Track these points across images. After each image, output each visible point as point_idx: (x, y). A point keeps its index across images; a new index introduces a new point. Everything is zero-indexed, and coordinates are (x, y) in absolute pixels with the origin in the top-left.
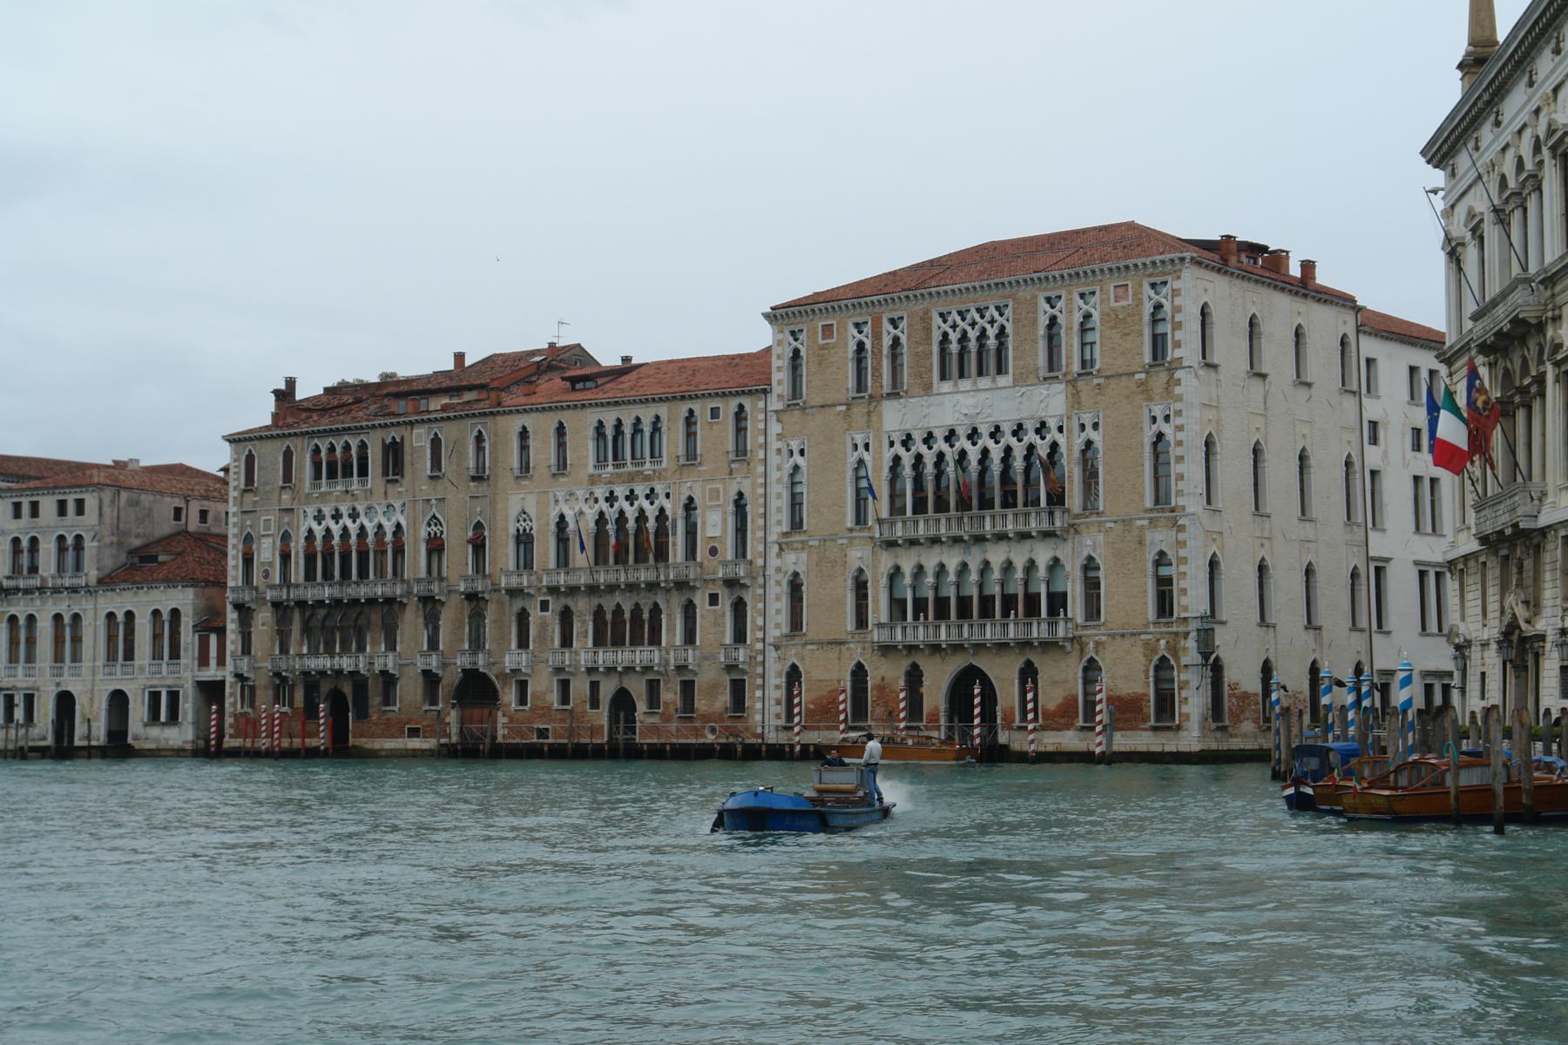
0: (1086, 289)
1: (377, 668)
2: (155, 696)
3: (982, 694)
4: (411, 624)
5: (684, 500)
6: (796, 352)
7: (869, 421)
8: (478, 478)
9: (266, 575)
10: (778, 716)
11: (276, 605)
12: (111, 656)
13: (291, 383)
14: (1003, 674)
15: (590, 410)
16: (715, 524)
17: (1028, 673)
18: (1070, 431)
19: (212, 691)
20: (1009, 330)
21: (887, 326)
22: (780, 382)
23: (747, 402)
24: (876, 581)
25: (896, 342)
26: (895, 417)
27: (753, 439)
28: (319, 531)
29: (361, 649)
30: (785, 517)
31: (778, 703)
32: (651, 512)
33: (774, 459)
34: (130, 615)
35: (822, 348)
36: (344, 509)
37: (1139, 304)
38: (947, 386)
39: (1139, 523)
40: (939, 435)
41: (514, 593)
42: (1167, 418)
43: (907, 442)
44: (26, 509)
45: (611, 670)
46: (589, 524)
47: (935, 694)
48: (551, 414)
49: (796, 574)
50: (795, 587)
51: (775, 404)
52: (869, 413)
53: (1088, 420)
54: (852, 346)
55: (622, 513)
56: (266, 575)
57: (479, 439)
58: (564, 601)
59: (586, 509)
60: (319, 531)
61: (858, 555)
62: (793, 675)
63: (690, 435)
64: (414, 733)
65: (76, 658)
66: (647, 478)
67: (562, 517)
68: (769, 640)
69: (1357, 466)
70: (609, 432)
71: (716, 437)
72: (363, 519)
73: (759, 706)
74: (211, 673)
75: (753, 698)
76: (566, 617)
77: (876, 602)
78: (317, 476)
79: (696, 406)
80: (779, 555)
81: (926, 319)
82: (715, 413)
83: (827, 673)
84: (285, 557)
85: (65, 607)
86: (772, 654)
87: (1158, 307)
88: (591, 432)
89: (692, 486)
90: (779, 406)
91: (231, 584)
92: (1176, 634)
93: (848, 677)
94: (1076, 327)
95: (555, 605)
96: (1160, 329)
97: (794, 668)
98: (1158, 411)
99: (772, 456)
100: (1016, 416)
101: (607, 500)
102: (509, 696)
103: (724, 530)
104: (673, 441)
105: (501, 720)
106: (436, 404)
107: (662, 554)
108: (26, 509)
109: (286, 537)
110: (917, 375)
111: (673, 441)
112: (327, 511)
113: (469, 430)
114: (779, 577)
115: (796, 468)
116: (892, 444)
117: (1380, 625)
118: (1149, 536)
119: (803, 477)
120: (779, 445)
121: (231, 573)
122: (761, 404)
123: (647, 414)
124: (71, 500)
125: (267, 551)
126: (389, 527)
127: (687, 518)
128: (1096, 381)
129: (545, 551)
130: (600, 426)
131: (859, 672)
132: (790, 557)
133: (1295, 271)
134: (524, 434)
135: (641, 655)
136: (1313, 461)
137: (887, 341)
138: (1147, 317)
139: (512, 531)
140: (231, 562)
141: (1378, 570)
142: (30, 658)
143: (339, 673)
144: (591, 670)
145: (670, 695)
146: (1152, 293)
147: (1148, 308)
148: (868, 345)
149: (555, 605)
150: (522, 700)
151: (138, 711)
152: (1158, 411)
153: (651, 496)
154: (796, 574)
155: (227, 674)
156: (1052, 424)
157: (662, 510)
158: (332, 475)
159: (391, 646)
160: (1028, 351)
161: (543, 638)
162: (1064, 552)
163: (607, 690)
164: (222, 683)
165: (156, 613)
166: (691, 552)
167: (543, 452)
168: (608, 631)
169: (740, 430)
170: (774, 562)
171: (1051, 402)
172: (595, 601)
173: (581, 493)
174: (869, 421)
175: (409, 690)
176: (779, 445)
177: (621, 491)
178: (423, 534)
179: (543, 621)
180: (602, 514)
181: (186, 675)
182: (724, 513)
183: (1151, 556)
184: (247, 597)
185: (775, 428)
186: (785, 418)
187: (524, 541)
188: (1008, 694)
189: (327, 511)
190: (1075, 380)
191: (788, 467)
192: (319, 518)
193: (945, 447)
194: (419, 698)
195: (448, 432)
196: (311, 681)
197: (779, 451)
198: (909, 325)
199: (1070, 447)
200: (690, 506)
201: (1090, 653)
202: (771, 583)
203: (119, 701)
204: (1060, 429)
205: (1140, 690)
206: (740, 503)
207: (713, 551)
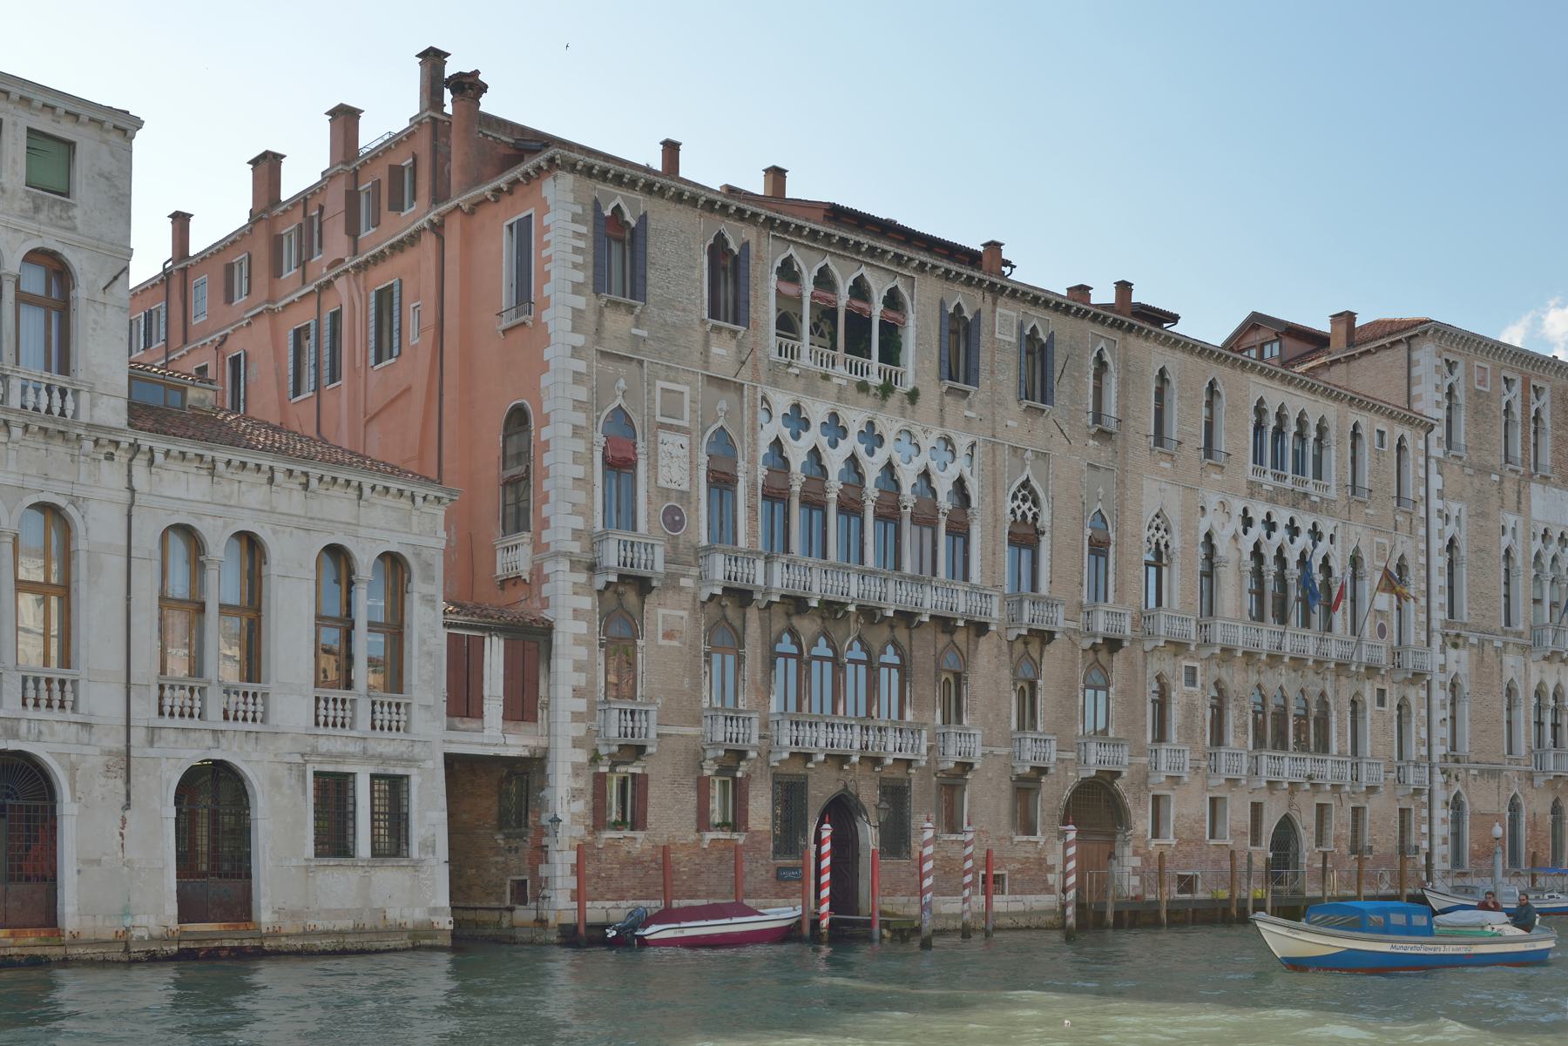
8: (1104, 435)
9: (673, 519)
15: (1254, 377)
31: (1445, 842)
33: (1436, 523)
48: (1202, 363)
62: (1456, 805)
66: (1314, 508)
68: (1436, 759)
80: (1443, 651)
102: (1142, 822)
114: (1442, 677)
126: (943, 485)
129: (1181, 581)
131: (1514, 807)
132: (1452, 652)
151: (280, 825)
168: (1274, 729)
173: (1237, 506)
175: (986, 801)
189: (817, 412)
194: (1005, 819)
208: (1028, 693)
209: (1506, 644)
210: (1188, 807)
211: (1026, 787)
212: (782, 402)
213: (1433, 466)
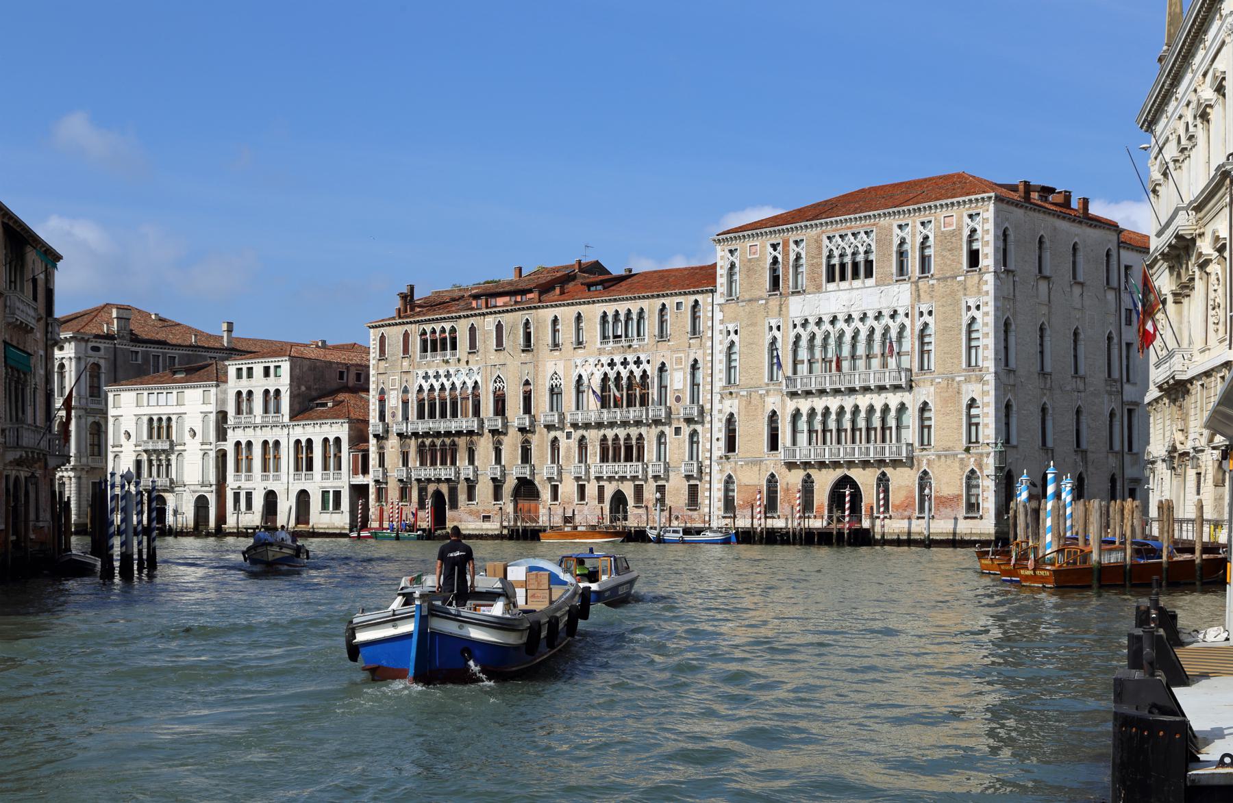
0: (925, 220)
1: (462, 477)
2: (325, 494)
3: (851, 494)
4: (484, 446)
5: (658, 365)
6: (733, 266)
7: (781, 310)
9: (394, 415)
10: (719, 509)
11: (400, 435)
12: (297, 468)
13: (412, 288)
14: (866, 479)
16: (678, 380)
17: (883, 481)
18: (913, 316)
19: (359, 491)
20: (873, 248)
21: (793, 246)
22: (722, 285)
23: (699, 297)
24: (784, 419)
25: (798, 257)
26: (798, 307)
27: (704, 324)
28: (426, 387)
29: (453, 463)
30: (723, 375)
32: (638, 373)
33: (718, 337)
34: (309, 441)
35: (750, 260)
36: (442, 372)
37: (960, 229)
38: (832, 286)
39: (958, 379)
40: (826, 319)
41: (550, 427)
42: (978, 307)
43: (805, 324)
44: (244, 373)
45: (610, 479)
46: (596, 383)
47: (821, 496)
49: (732, 415)
50: (730, 420)
51: (719, 299)
52: (781, 305)
53: (924, 309)
54: (770, 260)
55: (619, 373)
56: (394, 415)
57: (527, 323)
58: (581, 432)
59: (595, 370)
60: (426, 387)
61: (772, 402)
62: (729, 480)
63: (662, 322)
64: (486, 518)
65: (277, 469)
66: (635, 350)
67: (580, 376)
69: (1116, 340)
70: (610, 319)
71: (679, 322)
72: (454, 379)
73: (707, 502)
74: (360, 480)
75: (703, 495)
76: (582, 442)
77: (784, 433)
78: (424, 350)
79: (667, 301)
80: (721, 402)
81: (818, 241)
82: (679, 305)
83: (751, 479)
84: (405, 403)
85: (271, 435)
86: (715, 467)
87: (974, 231)
88: (598, 320)
89: (663, 354)
90: (722, 301)
91: (372, 421)
92: (982, 454)
93: (765, 483)
94: (918, 245)
95: (576, 435)
96: (975, 246)
97: (730, 477)
98: (972, 303)
99: (716, 333)
100: (877, 306)
101: (609, 365)
102: (546, 494)
103: (685, 385)
104: (651, 325)
105: (543, 511)
106: (500, 301)
107: (644, 401)
108: (244, 373)
109: (406, 391)
110: (813, 279)
111: (651, 325)
112: (431, 373)
113: (518, 318)
114: (720, 416)
115: (732, 343)
116: (795, 326)
117: (1130, 448)
118: (964, 387)
119: (736, 349)
120: (721, 327)
121: (372, 414)
122: (710, 300)
123: (635, 306)
124: (245, 368)
125: (393, 401)
127: (660, 378)
128: (931, 282)
130: (605, 315)
131: (772, 480)
132: (727, 402)
133: (1075, 204)
134: (555, 321)
135: (629, 469)
136: (1082, 336)
137: (792, 257)
138: (965, 238)
139: (548, 386)
140: (371, 407)
141: (1130, 411)
142: (249, 469)
143: (439, 481)
144: (599, 479)
145: (650, 493)
146: (969, 221)
147: (966, 232)
148: (780, 260)
149: (576, 435)
150: (555, 497)
152: (972, 303)
153: (638, 362)
154: (732, 415)
155: (369, 480)
156: (901, 311)
157: (645, 372)
158: (434, 349)
159: (471, 461)
160: (886, 265)
161: (568, 458)
162: (906, 397)
163: (609, 490)
164: (367, 486)
165: (298, 442)
166: (662, 400)
167: (567, 334)
169: (695, 318)
170: (717, 406)
171: (900, 295)
172: (602, 432)
173: (592, 361)
174: (781, 310)
175: (484, 489)
176: (721, 327)
177: (618, 359)
178: (491, 388)
179: (568, 446)
180: (606, 374)
181: (343, 481)
182: (685, 373)
183: (965, 401)
184: (380, 431)
185: (718, 316)
186: (726, 308)
187: (555, 392)
188: (869, 495)
189: (431, 373)
190: (917, 282)
191: (726, 343)
192: (426, 377)
193: (830, 328)
195: (506, 319)
196: (423, 484)
197: (721, 331)
198: (807, 245)
199: (913, 327)
200: (662, 368)
201: (925, 467)
202: (715, 420)
203: (303, 496)
204: (907, 315)
205: (957, 493)
206: (694, 366)
207: (678, 399)
208: (498, 452)
209: (768, 392)
210: (568, 488)
211: (497, 484)
212: (421, 373)
213: (717, 308)
